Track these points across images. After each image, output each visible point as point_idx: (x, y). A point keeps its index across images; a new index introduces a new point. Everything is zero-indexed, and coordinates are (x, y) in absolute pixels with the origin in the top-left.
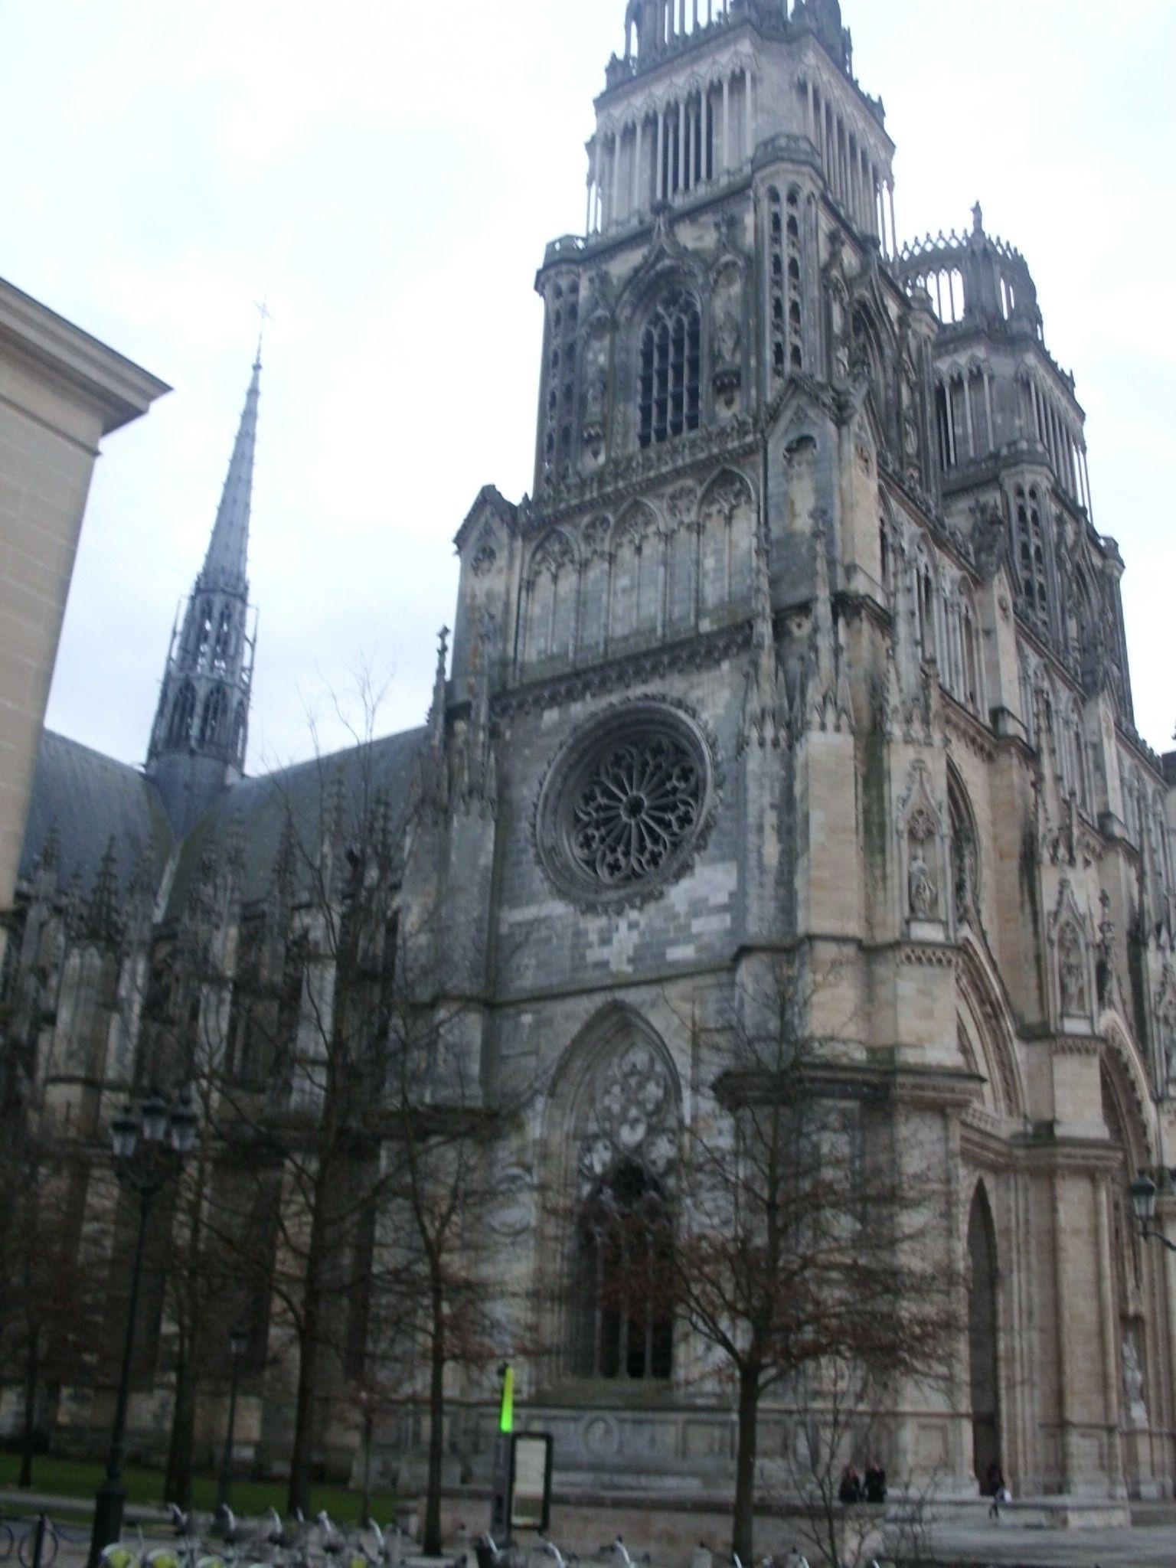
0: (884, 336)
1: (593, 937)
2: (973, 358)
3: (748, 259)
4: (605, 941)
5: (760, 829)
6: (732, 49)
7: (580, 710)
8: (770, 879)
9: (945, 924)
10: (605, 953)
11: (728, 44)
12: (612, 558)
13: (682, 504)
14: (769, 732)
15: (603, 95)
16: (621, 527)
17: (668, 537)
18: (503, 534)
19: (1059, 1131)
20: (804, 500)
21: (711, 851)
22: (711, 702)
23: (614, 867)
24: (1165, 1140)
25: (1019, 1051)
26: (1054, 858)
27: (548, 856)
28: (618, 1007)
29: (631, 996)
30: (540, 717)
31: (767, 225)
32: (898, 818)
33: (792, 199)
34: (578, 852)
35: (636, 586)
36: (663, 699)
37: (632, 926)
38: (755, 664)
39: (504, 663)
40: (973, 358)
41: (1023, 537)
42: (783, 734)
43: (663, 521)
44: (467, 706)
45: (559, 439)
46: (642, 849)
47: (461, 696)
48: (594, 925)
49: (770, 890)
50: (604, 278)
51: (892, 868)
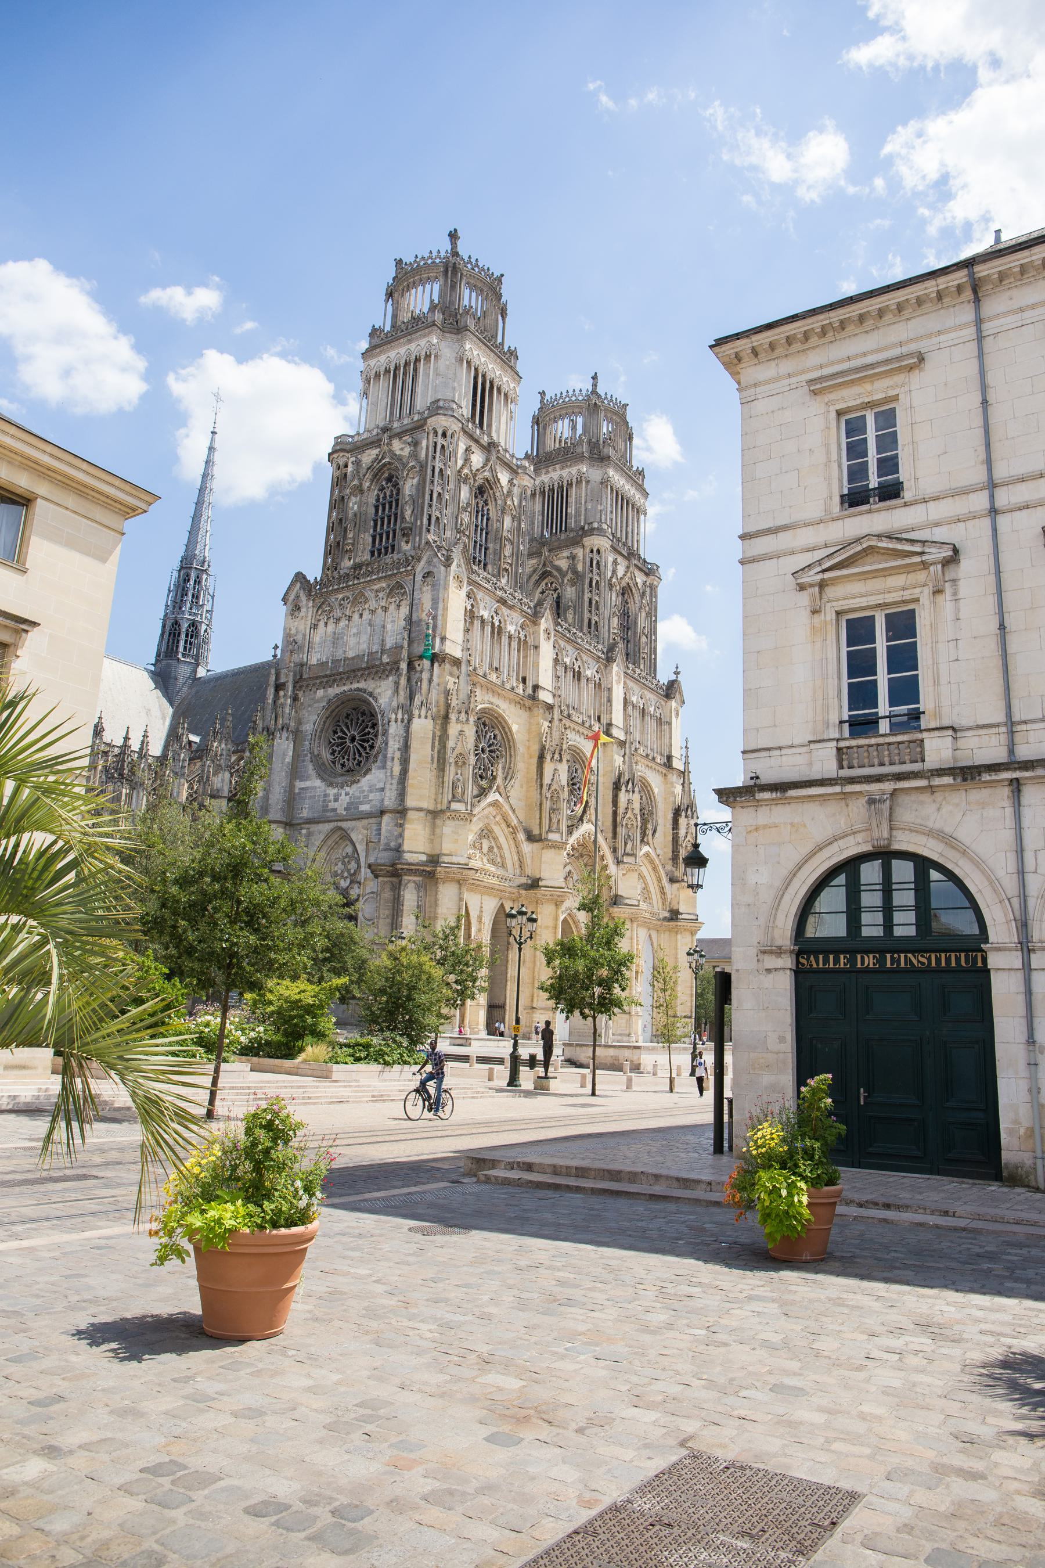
0: (498, 494)
1: (332, 798)
2: (579, 471)
3: (421, 466)
4: (336, 800)
5: (393, 759)
6: (427, 339)
7: (334, 691)
8: (395, 781)
9: (466, 804)
10: (336, 805)
11: (425, 336)
12: (350, 618)
13: (381, 595)
14: (400, 716)
15: (367, 351)
16: (355, 602)
17: (373, 612)
18: (303, 598)
19: (540, 883)
20: (427, 605)
21: (378, 763)
22: (384, 694)
23: (343, 765)
24: (620, 882)
25: (527, 848)
26: (552, 758)
27: (316, 759)
28: (340, 828)
29: (344, 825)
30: (315, 692)
31: (431, 449)
32: (451, 757)
33: (444, 435)
34: (329, 756)
35: (358, 634)
36: (364, 691)
37: (347, 794)
38: (397, 684)
39: (302, 665)
40: (579, 471)
41: (590, 575)
42: (406, 716)
43: (372, 604)
44: (284, 684)
45: (334, 549)
46: (354, 759)
47: (282, 680)
48: (332, 792)
49: (395, 786)
50: (358, 463)
51: (446, 779)
